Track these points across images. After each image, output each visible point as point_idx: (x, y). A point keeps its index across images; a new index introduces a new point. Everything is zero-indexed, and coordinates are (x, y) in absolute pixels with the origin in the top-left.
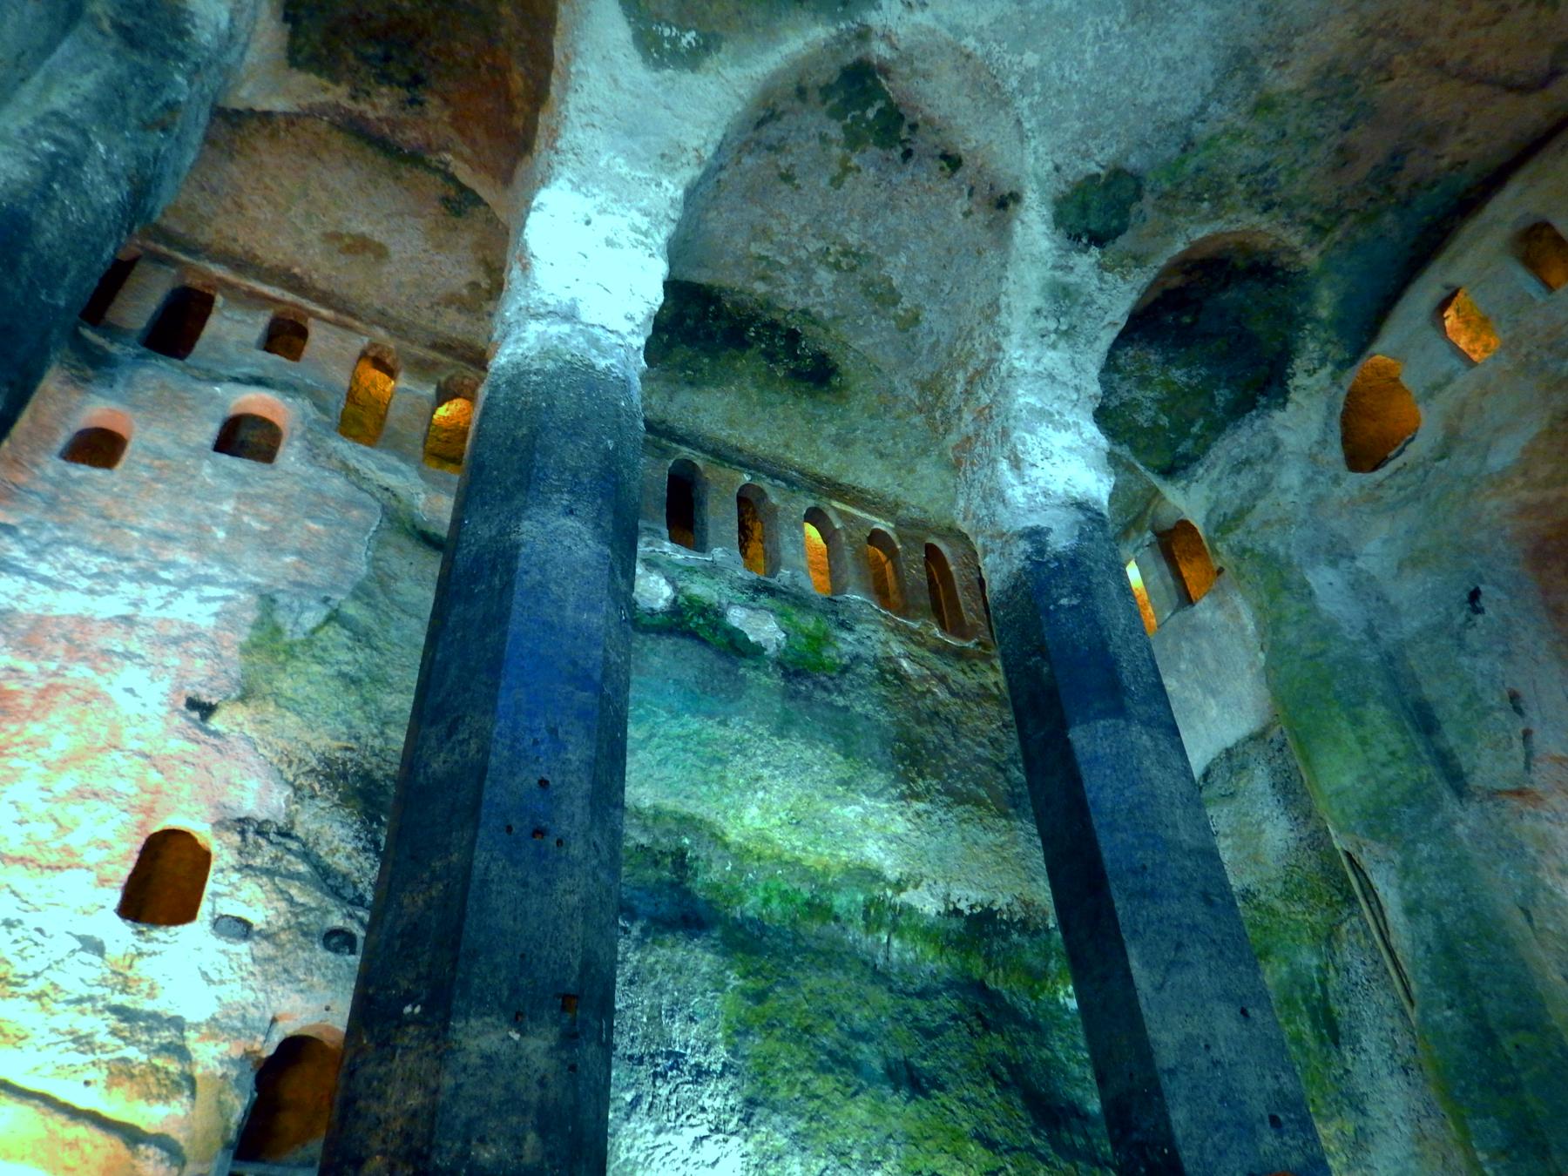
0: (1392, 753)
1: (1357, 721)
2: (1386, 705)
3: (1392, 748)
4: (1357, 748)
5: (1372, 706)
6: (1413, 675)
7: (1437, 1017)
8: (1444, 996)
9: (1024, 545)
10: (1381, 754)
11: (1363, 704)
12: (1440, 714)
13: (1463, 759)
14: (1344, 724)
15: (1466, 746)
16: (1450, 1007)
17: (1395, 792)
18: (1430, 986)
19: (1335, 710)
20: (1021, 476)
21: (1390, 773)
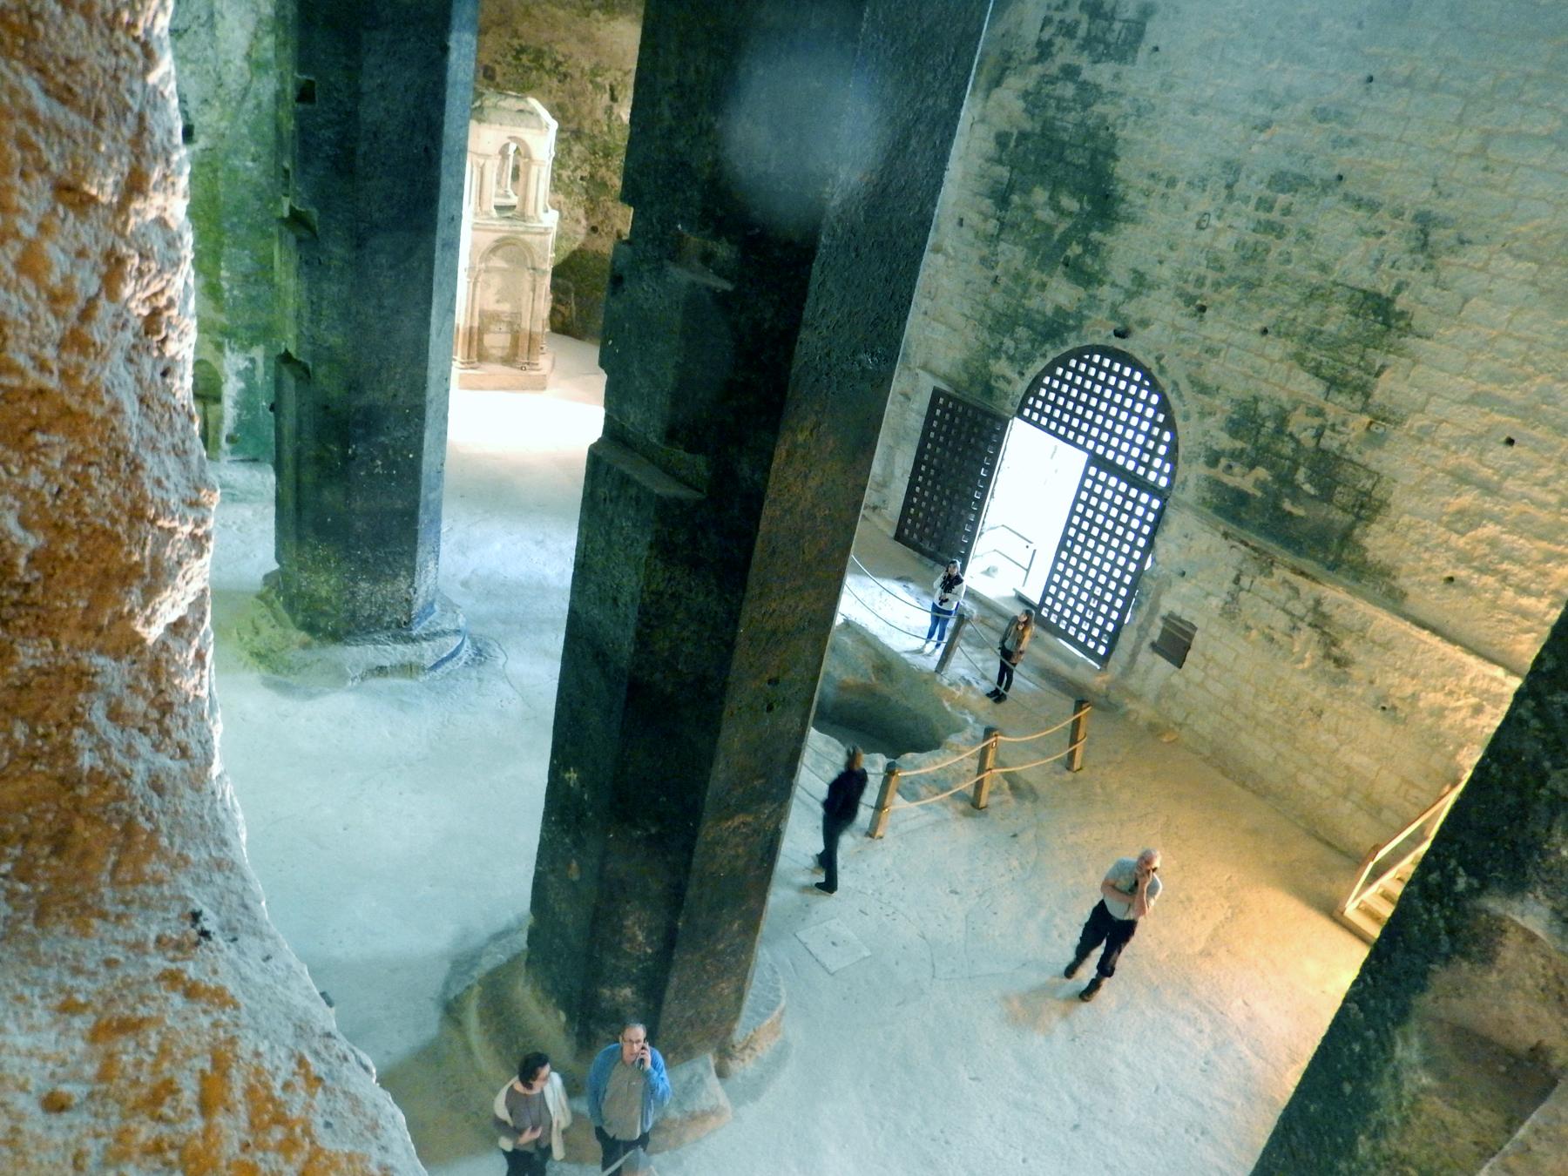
7: (237, 163)
8: (253, 149)
16: (254, 160)
18: (243, 136)
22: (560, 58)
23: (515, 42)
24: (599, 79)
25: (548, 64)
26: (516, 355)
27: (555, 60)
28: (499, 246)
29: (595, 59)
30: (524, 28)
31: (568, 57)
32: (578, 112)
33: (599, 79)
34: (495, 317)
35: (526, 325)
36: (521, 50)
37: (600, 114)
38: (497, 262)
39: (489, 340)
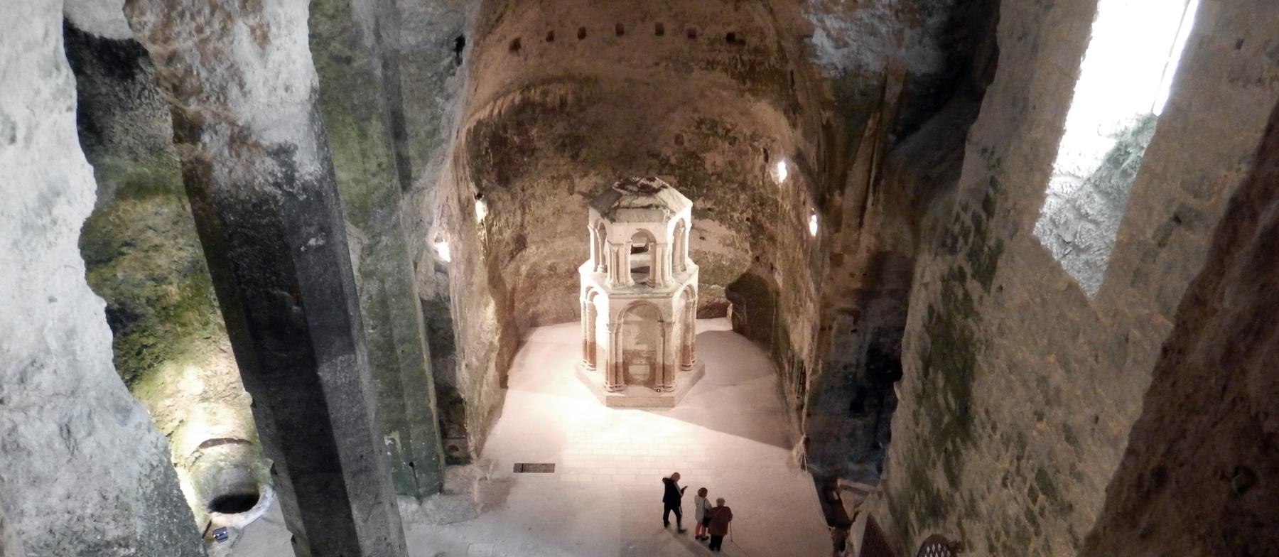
0: (379, 165)
1: (363, 135)
2: (384, 123)
3: (380, 160)
4: (359, 158)
5: (374, 122)
6: (400, 87)
9: (270, 163)
10: (372, 165)
11: (369, 119)
12: (409, 129)
13: (414, 169)
14: (354, 134)
15: (420, 162)
17: (375, 197)
19: (349, 119)
20: (263, 55)
21: (375, 181)
22: (729, 126)
23: (696, 116)
24: (756, 144)
25: (720, 131)
26: (654, 380)
27: (724, 128)
28: (633, 307)
29: (752, 128)
30: (701, 104)
31: (734, 126)
32: (743, 168)
33: (756, 144)
34: (637, 354)
35: (660, 360)
36: (701, 122)
37: (757, 171)
38: (633, 317)
39: (633, 370)
